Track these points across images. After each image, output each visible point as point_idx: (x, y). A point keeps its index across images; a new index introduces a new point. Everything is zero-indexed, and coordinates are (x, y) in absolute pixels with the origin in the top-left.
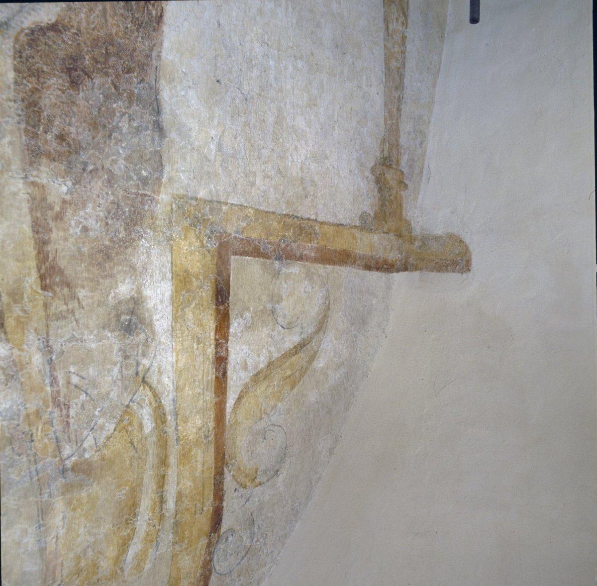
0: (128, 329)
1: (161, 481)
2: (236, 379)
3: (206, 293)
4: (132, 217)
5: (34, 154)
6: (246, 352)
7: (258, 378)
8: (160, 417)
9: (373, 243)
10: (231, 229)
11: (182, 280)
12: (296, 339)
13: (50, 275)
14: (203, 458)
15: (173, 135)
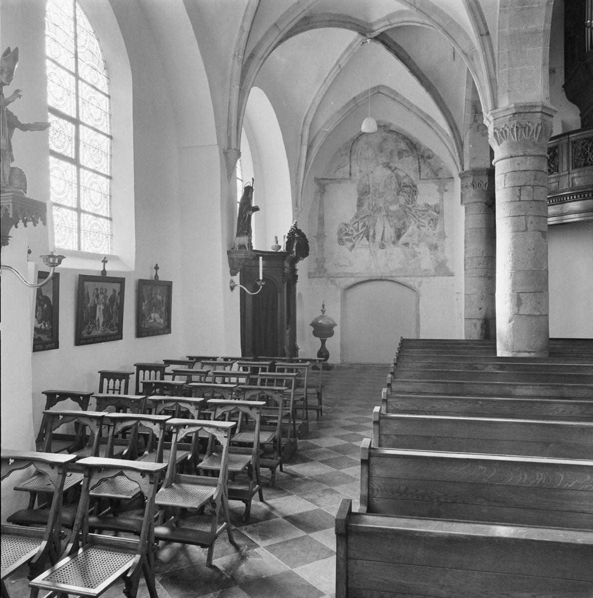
0: (361, 171)
1: (357, 157)
2: (348, 166)
3: (352, 174)
4: (360, 181)
5: (369, 185)
6: (347, 168)
7: (345, 166)
8: (357, 162)
9: (325, 182)
10: (349, 181)
11: (355, 175)
12: (340, 170)
13: (368, 175)
14: (352, 158)
15: (356, 189)
